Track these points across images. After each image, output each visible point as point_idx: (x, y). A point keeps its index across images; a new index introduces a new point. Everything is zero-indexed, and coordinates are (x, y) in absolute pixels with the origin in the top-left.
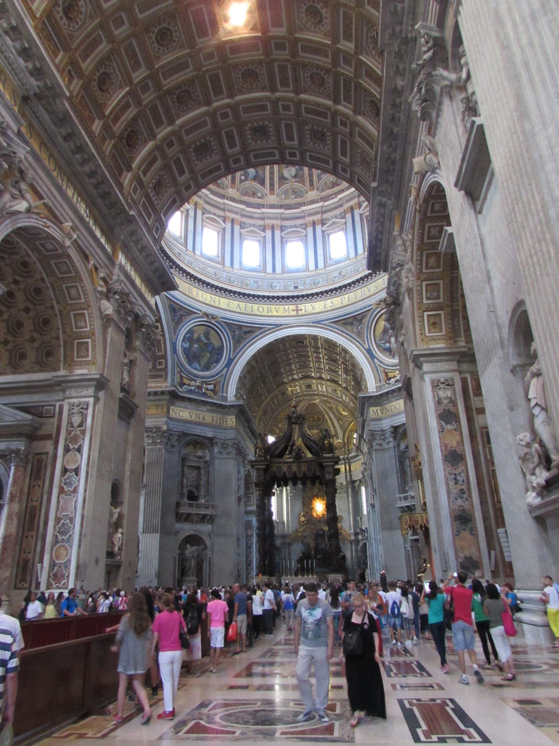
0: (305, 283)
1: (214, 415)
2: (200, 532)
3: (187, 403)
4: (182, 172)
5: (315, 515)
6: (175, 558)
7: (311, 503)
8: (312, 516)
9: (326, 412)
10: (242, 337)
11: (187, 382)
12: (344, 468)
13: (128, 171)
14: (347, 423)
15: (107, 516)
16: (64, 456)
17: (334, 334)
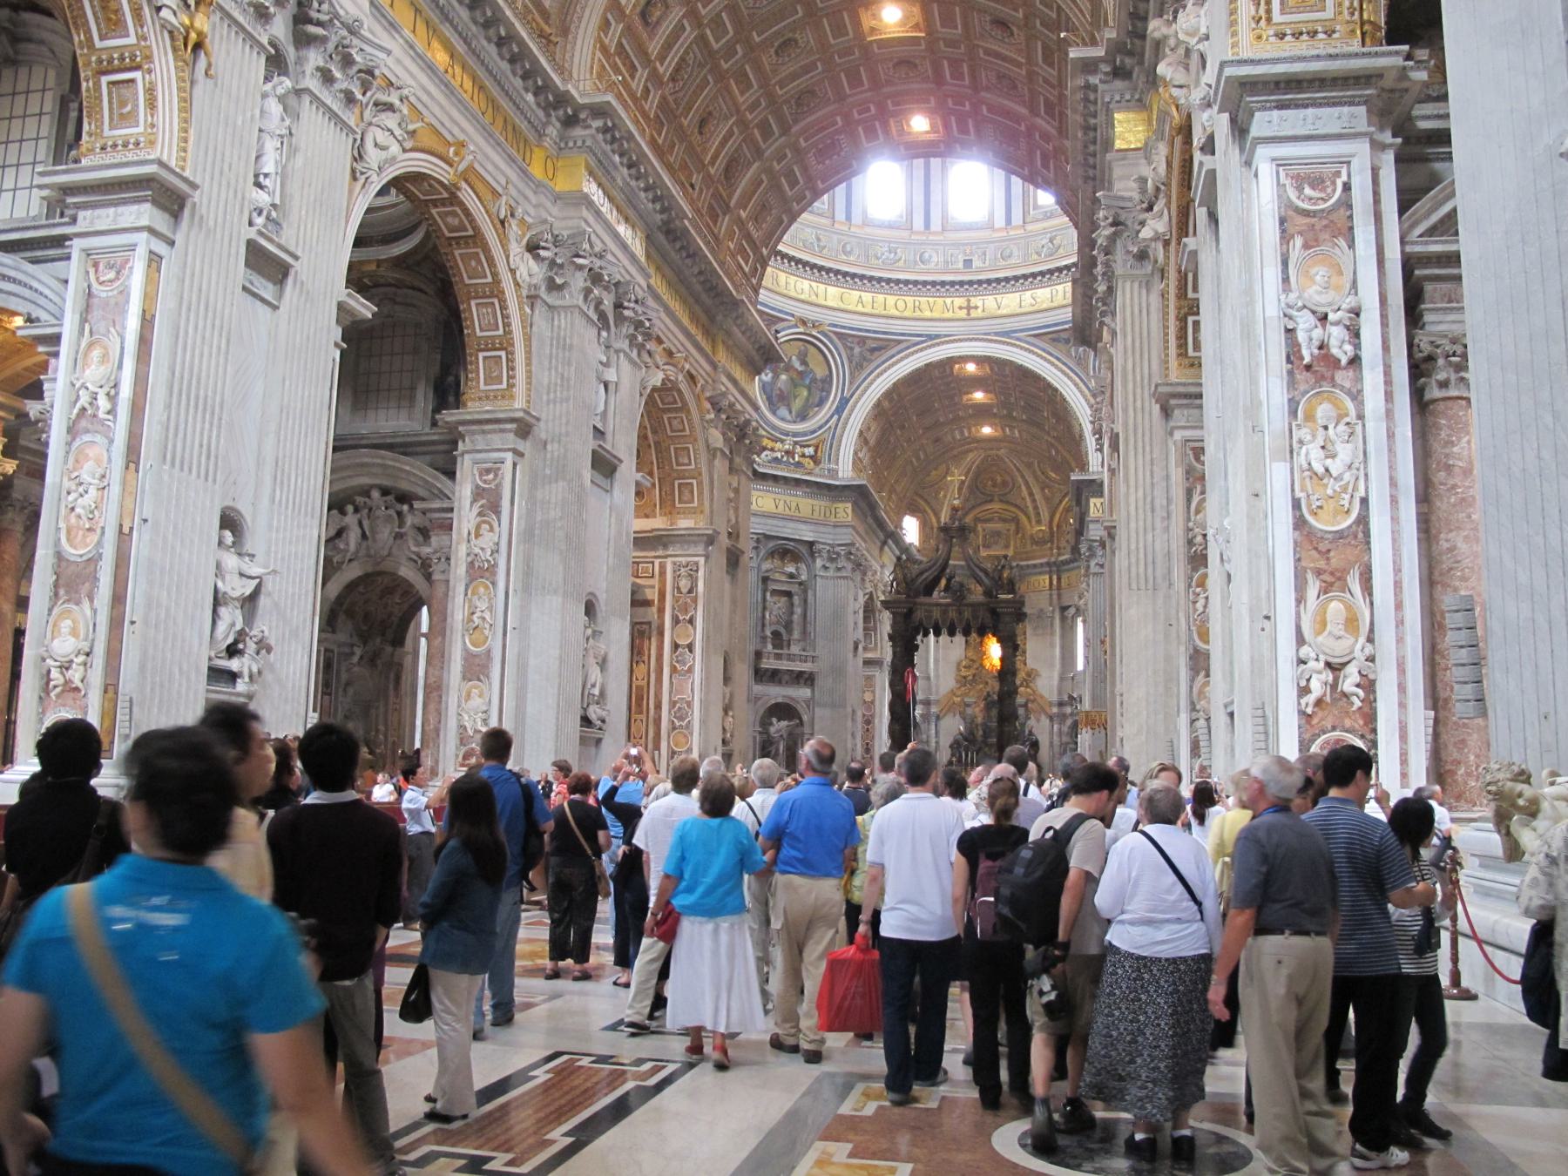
0: (985, 254)
1: (815, 502)
2: (793, 699)
3: (770, 483)
4: (793, 183)
5: (988, 665)
6: (755, 738)
7: (981, 644)
8: (982, 666)
9: (1018, 470)
10: (865, 359)
11: (770, 444)
12: (1047, 581)
13: (725, 214)
14: (1058, 496)
15: (721, 696)
16: (673, 629)
17: (1034, 357)
